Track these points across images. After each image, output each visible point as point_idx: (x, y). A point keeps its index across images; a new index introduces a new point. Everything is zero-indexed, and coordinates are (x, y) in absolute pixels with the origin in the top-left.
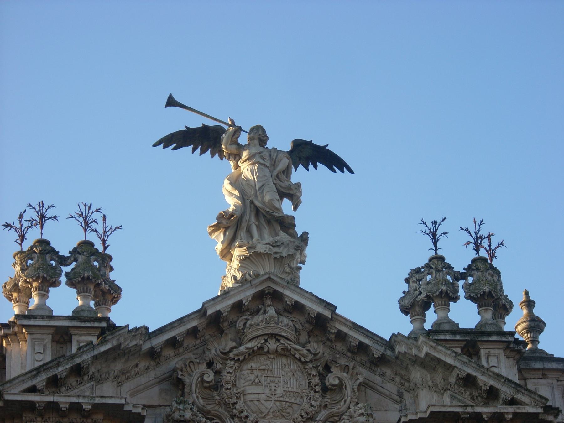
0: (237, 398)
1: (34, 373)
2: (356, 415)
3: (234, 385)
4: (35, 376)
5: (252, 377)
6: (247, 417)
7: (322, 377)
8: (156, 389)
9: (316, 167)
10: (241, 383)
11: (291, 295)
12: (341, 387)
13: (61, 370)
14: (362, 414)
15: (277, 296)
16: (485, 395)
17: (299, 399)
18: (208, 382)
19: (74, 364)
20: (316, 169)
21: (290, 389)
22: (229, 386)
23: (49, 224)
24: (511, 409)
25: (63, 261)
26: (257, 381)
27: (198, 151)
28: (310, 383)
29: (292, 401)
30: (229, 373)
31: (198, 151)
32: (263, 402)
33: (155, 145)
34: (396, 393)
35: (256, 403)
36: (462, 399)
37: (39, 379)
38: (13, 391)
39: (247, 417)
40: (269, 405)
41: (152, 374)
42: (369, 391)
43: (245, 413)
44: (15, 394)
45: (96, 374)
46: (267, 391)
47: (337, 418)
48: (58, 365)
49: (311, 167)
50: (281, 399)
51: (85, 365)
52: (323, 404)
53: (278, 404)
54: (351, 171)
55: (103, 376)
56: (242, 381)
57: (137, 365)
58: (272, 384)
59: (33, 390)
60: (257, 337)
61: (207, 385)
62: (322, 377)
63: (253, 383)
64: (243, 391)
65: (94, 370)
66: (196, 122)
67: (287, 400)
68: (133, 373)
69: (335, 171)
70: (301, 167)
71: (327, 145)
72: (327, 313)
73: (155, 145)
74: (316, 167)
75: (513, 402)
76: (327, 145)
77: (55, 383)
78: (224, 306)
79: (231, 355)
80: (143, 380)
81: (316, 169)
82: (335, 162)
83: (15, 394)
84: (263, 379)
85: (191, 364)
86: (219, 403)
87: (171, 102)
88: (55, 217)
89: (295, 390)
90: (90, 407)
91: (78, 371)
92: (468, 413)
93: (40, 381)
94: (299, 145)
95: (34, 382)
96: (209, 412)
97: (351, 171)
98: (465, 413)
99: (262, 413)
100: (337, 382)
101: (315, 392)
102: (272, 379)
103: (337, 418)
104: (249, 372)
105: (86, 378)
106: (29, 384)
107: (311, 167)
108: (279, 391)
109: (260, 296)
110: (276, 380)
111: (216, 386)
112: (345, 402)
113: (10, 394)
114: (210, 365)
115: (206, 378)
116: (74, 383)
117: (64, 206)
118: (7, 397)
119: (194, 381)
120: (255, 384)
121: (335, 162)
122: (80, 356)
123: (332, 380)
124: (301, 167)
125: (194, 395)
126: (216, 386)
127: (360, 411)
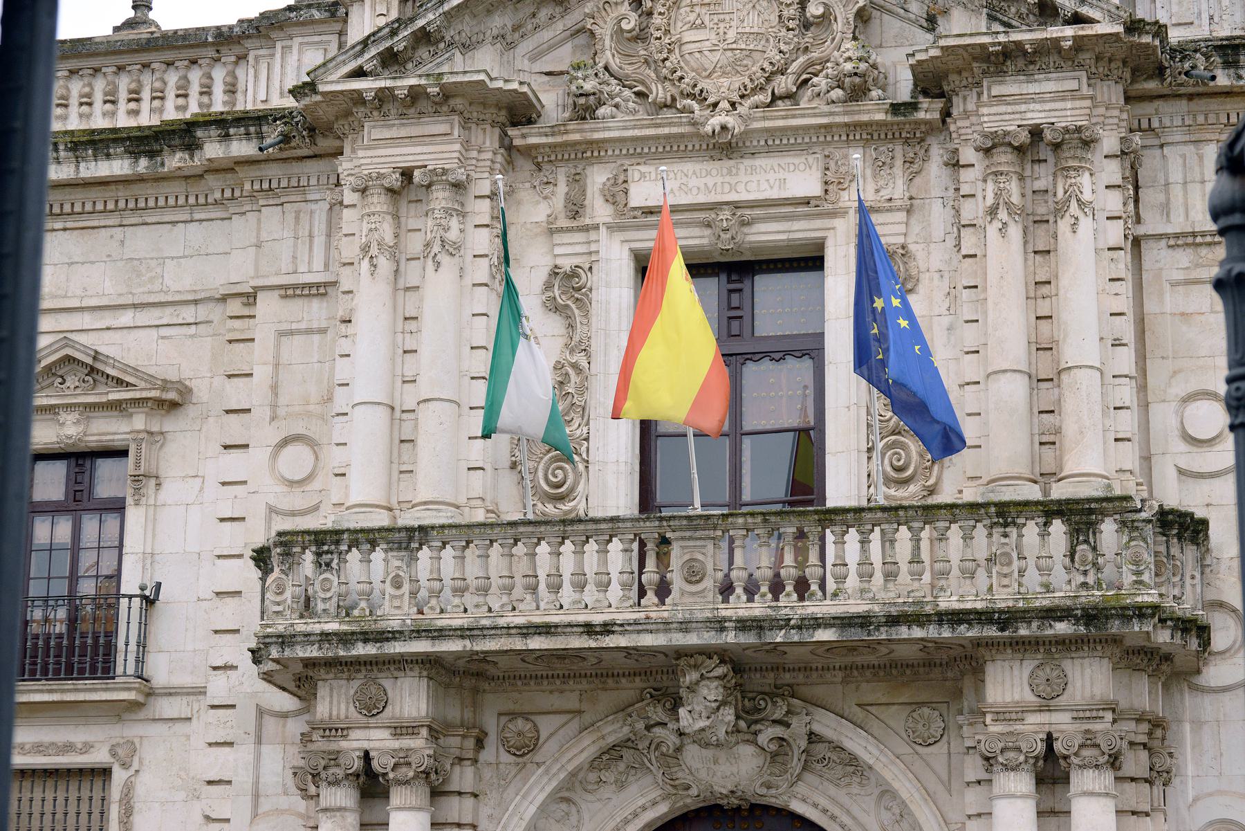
0: (670, 51)
1: (358, 48)
2: (841, 60)
3: (667, 32)
4: (362, 52)
5: (692, 17)
6: (681, 78)
8: (568, 47)
10: (678, 28)
12: (826, 19)
13: (400, 42)
14: (850, 59)
16: (1036, 11)
17: (763, 42)
18: (630, 31)
19: (415, 28)
21: (748, 30)
22: (658, 34)
24: (1069, 31)
26: (698, 22)
28: (780, 16)
29: (751, 47)
30: (660, 14)
32: (707, 53)
34: (925, 16)
35: (697, 55)
36: (1006, 19)
37: (367, 56)
38: (330, 78)
39: (681, 78)
40: (717, 56)
41: (560, 26)
42: (886, 17)
43: (679, 74)
44: (332, 82)
45: (457, 38)
46: (713, 36)
47: (818, 67)
48: (394, 33)
50: (734, 46)
51: (430, 29)
52: (802, 46)
53: (729, 54)
55: (474, 39)
56: (679, 24)
57: (534, 15)
58: (722, 25)
59: (359, 73)
61: (629, 35)
63: (694, 26)
64: (679, 40)
65: (452, 33)
67: (743, 46)
68: (530, 27)
75: (1077, 19)
77: (390, 60)
80: (546, 35)
83: (332, 82)
84: (707, 19)
85: (607, 6)
86: (646, 62)
89: (756, 30)
90: (437, 89)
91: (424, 37)
92: (999, 43)
93: (367, 59)
95: (360, 61)
96: (627, 76)
98: (994, 44)
99: (705, 70)
100: (820, 11)
101: (789, 30)
102: (722, 17)
103: (818, 67)
104: (688, 9)
105: (442, 45)
106: (352, 65)
108: (731, 35)
110: (727, 17)
111: (641, 36)
112: (833, 39)
113: (327, 83)
115: (626, 26)
116: (425, 55)
118: (321, 88)
119: (609, 33)
120: (696, 28)
122: (424, 16)
125: (608, 53)
126: (641, 36)
127: (846, 55)
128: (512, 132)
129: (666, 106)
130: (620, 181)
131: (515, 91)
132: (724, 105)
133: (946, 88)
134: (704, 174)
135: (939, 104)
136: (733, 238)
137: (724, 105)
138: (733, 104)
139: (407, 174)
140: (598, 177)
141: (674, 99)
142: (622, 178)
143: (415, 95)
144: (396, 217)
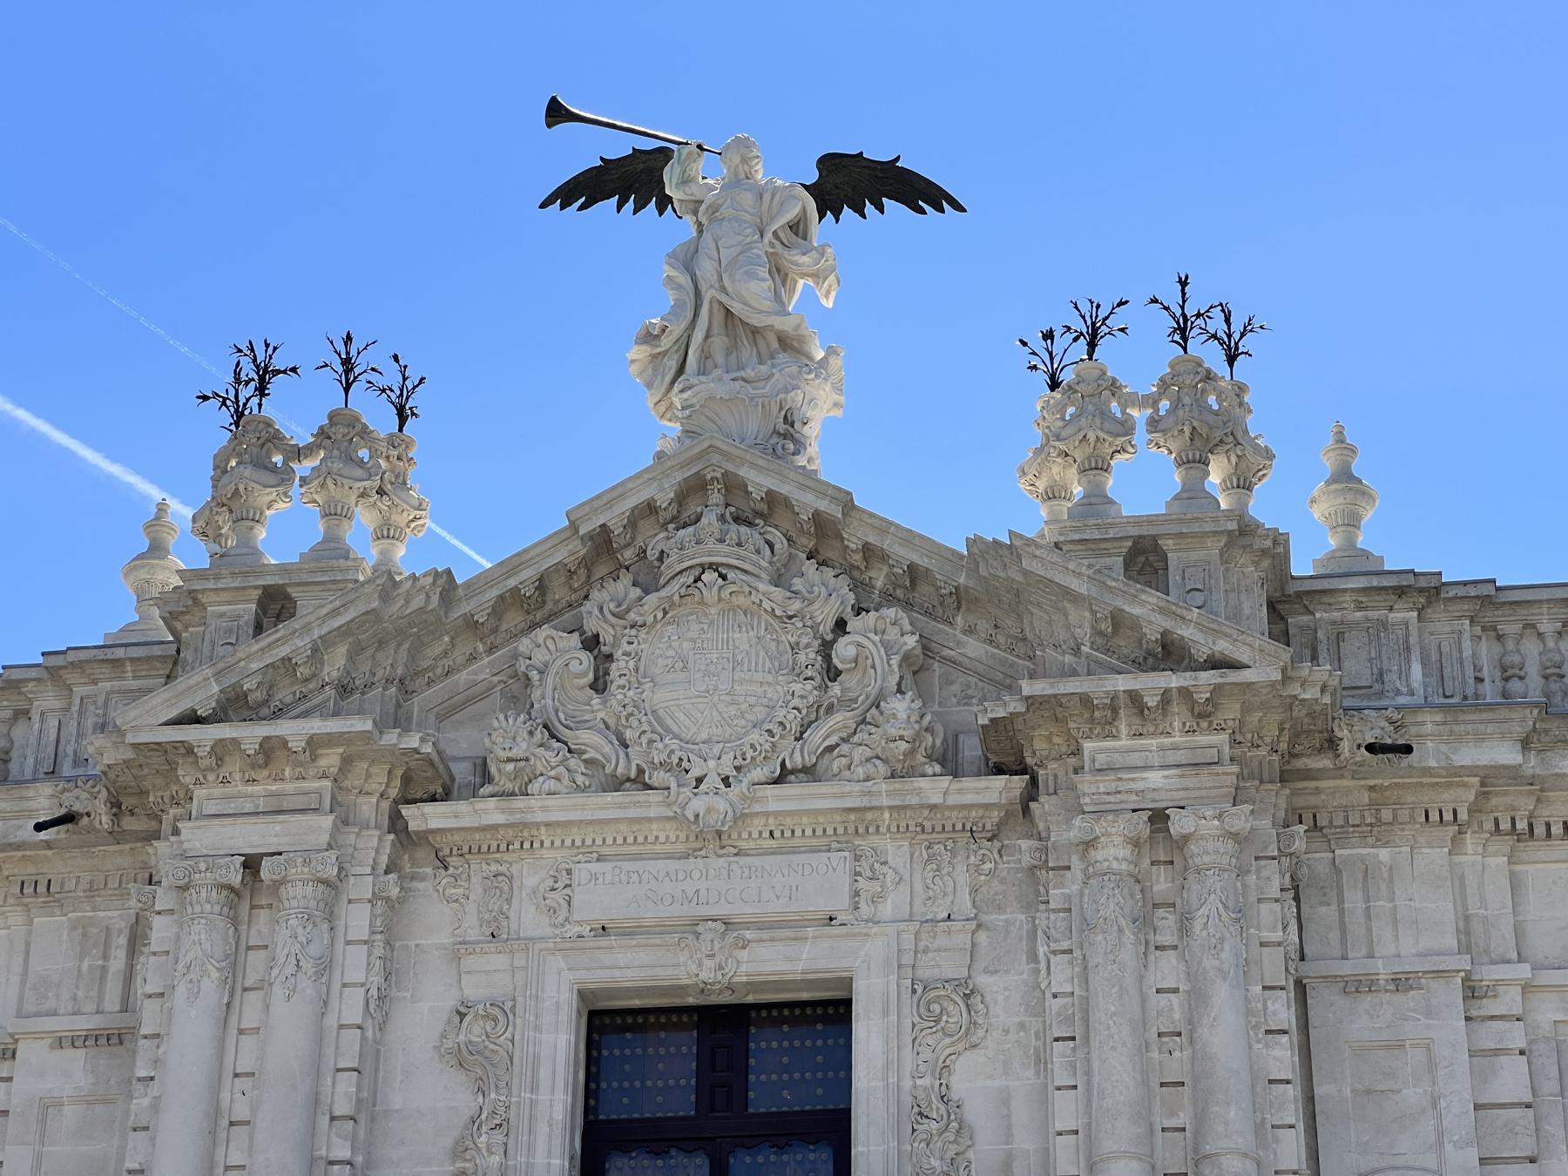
7: (826, 649)
9: (881, 209)
11: (759, 480)
15: (733, 486)
20: (882, 212)
23: (276, 385)
24: (1208, 677)
25: (298, 453)
27: (630, 205)
31: (630, 205)
33: (543, 206)
49: (869, 208)
54: (959, 207)
59: (192, 718)
60: (680, 572)
62: (826, 649)
66: (619, 147)
69: (923, 212)
70: (847, 211)
71: (898, 159)
72: (836, 511)
73: (543, 206)
74: (881, 209)
76: (898, 159)
78: (614, 517)
79: (632, 616)
81: (882, 212)
82: (920, 193)
87: (556, 113)
88: (294, 370)
94: (830, 163)
97: (959, 207)
100: (851, 651)
107: (869, 208)
109: (695, 488)
114: (592, 643)
117: (304, 347)
121: (920, 193)
123: (844, 650)
124: (847, 211)
128: (406, 811)
129: (629, 780)
130: (560, 885)
131: (416, 751)
132: (713, 781)
133: (1029, 761)
134: (681, 876)
135: (1019, 782)
136: (721, 968)
137: (713, 781)
138: (726, 781)
139: (251, 864)
140: (531, 875)
141: (641, 771)
142: (564, 880)
143: (270, 750)
144: (235, 922)
